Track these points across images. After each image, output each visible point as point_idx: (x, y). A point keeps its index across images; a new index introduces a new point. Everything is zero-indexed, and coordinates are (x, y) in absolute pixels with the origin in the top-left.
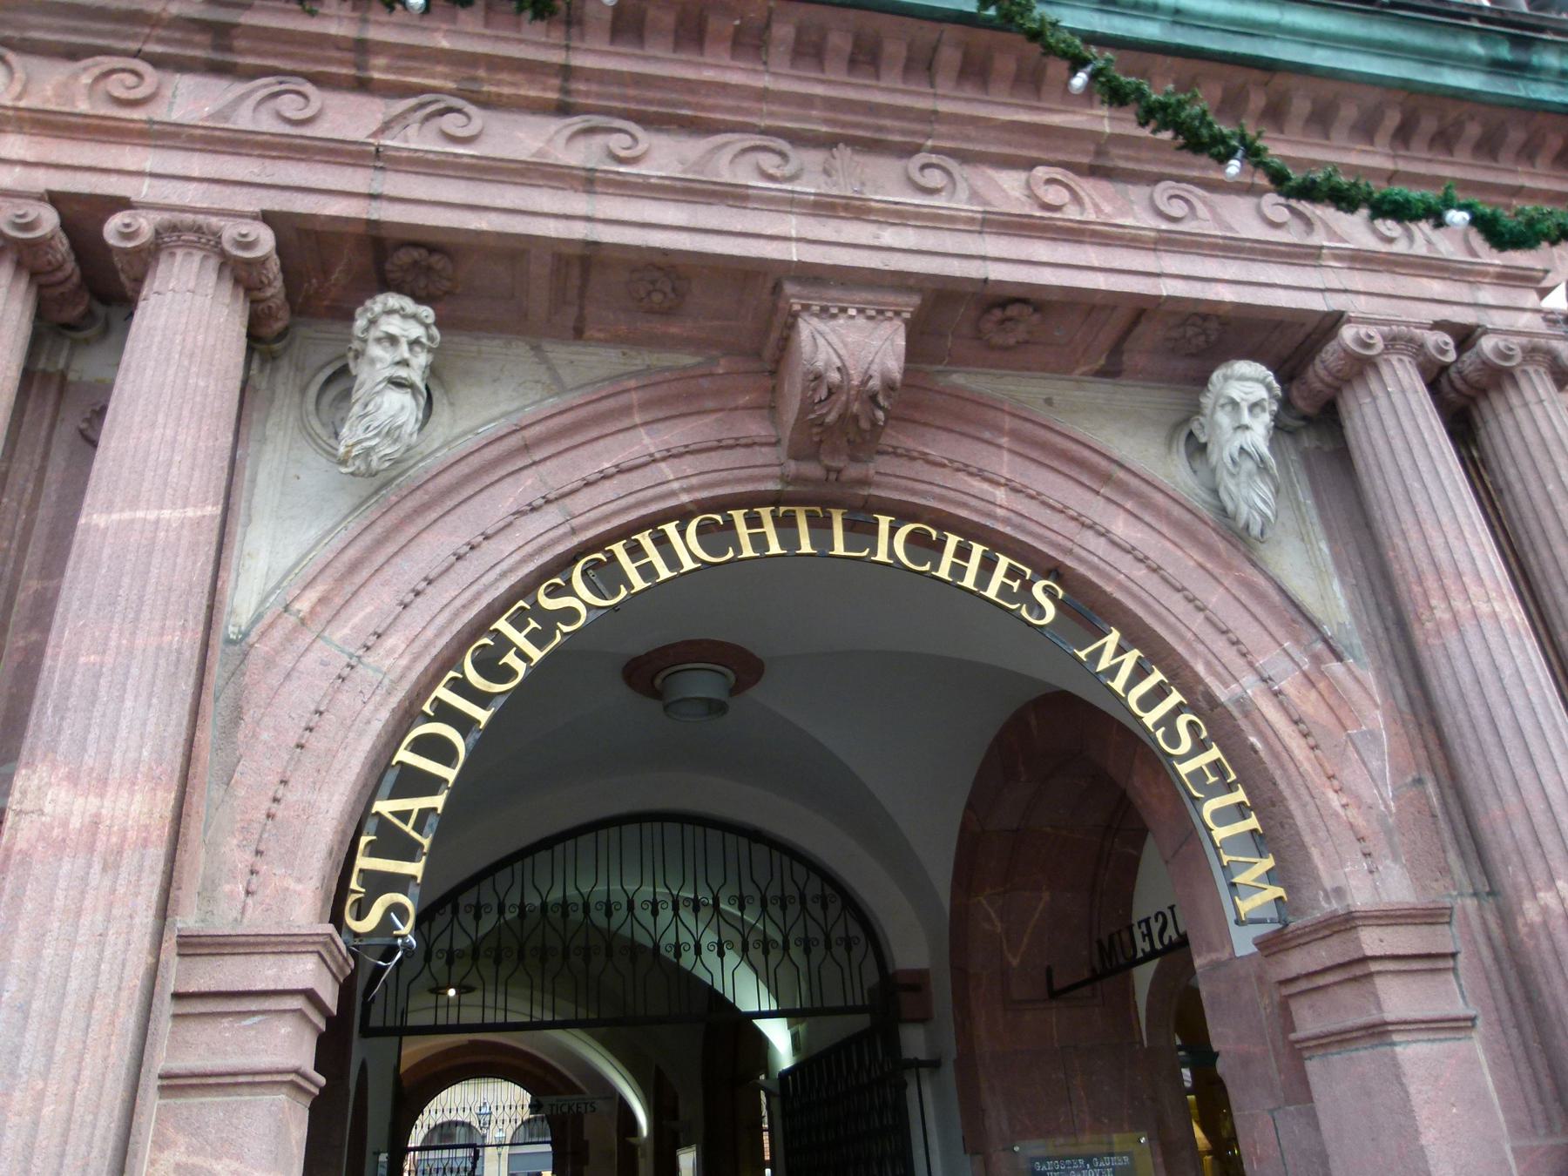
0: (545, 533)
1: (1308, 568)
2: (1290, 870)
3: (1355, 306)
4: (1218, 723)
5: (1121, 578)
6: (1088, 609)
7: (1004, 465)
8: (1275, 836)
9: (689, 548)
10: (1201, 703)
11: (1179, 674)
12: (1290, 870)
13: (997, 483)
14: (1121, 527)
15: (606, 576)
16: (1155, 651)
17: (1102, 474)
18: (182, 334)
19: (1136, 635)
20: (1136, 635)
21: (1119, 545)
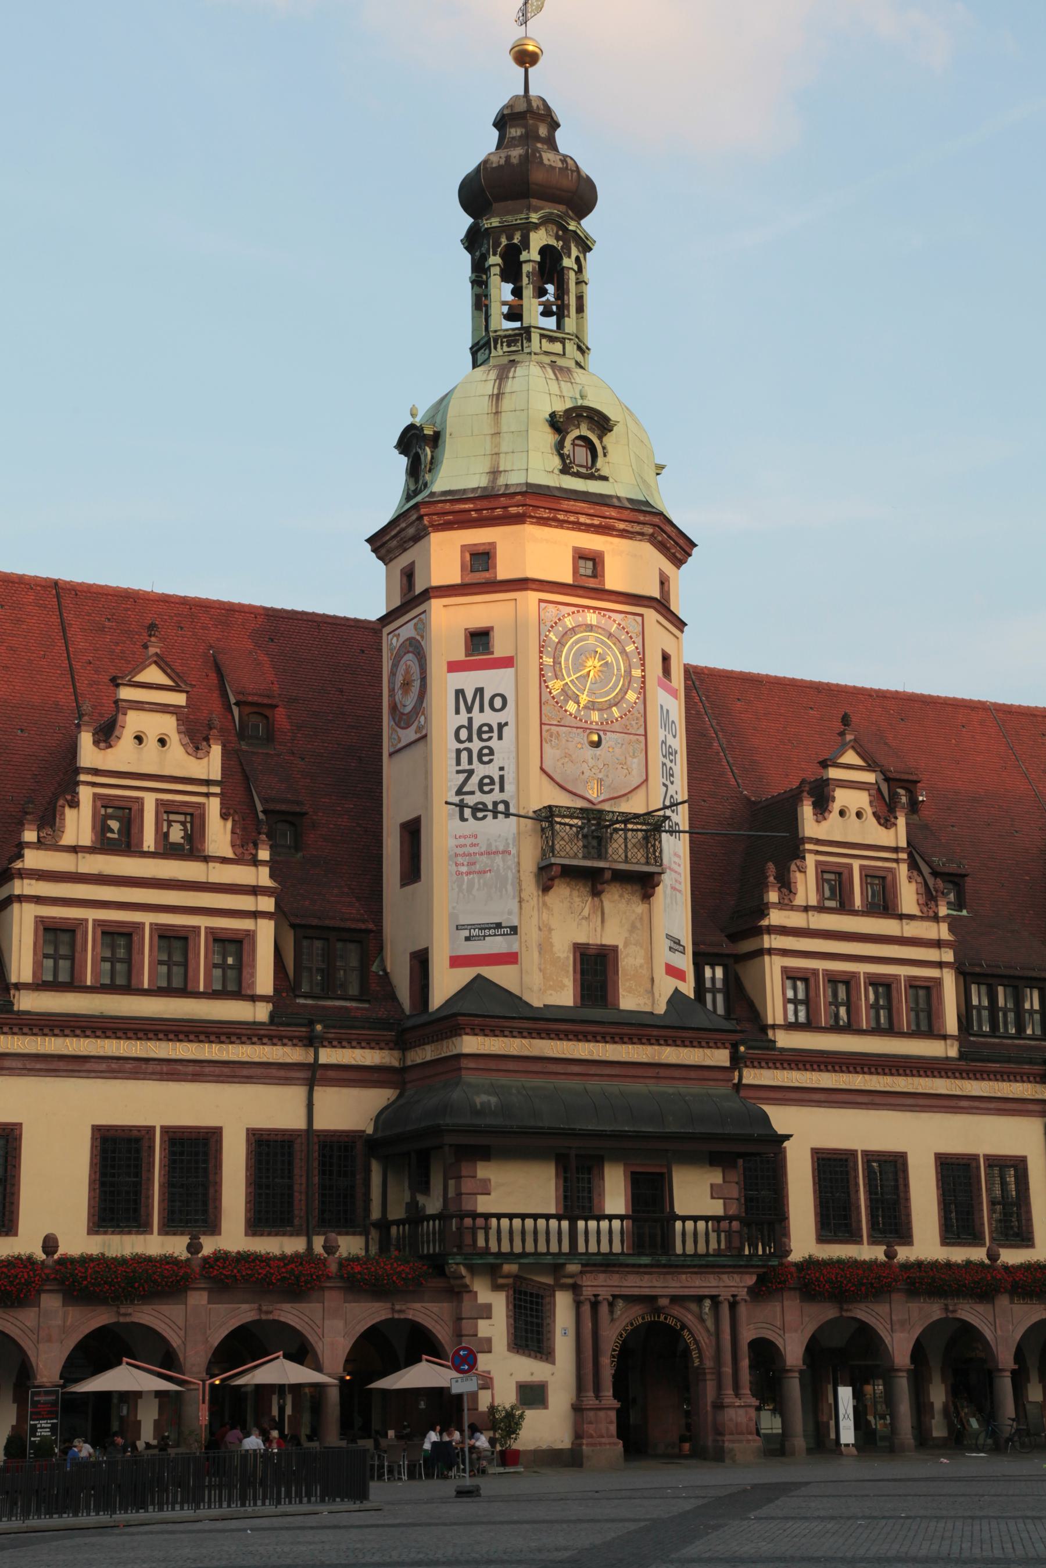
0: (627, 1320)
1: (710, 1324)
2: (701, 1361)
3: (722, 1294)
4: (696, 1342)
5: (689, 1323)
6: (684, 1326)
7: (677, 1308)
8: (700, 1357)
9: (641, 1321)
10: (695, 1339)
11: (693, 1336)
12: (701, 1361)
13: (677, 1311)
14: (690, 1317)
15: (632, 1324)
16: (690, 1333)
17: (688, 1310)
18: (604, 1309)
19: (689, 1330)
20: (689, 1330)
21: (689, 1319)
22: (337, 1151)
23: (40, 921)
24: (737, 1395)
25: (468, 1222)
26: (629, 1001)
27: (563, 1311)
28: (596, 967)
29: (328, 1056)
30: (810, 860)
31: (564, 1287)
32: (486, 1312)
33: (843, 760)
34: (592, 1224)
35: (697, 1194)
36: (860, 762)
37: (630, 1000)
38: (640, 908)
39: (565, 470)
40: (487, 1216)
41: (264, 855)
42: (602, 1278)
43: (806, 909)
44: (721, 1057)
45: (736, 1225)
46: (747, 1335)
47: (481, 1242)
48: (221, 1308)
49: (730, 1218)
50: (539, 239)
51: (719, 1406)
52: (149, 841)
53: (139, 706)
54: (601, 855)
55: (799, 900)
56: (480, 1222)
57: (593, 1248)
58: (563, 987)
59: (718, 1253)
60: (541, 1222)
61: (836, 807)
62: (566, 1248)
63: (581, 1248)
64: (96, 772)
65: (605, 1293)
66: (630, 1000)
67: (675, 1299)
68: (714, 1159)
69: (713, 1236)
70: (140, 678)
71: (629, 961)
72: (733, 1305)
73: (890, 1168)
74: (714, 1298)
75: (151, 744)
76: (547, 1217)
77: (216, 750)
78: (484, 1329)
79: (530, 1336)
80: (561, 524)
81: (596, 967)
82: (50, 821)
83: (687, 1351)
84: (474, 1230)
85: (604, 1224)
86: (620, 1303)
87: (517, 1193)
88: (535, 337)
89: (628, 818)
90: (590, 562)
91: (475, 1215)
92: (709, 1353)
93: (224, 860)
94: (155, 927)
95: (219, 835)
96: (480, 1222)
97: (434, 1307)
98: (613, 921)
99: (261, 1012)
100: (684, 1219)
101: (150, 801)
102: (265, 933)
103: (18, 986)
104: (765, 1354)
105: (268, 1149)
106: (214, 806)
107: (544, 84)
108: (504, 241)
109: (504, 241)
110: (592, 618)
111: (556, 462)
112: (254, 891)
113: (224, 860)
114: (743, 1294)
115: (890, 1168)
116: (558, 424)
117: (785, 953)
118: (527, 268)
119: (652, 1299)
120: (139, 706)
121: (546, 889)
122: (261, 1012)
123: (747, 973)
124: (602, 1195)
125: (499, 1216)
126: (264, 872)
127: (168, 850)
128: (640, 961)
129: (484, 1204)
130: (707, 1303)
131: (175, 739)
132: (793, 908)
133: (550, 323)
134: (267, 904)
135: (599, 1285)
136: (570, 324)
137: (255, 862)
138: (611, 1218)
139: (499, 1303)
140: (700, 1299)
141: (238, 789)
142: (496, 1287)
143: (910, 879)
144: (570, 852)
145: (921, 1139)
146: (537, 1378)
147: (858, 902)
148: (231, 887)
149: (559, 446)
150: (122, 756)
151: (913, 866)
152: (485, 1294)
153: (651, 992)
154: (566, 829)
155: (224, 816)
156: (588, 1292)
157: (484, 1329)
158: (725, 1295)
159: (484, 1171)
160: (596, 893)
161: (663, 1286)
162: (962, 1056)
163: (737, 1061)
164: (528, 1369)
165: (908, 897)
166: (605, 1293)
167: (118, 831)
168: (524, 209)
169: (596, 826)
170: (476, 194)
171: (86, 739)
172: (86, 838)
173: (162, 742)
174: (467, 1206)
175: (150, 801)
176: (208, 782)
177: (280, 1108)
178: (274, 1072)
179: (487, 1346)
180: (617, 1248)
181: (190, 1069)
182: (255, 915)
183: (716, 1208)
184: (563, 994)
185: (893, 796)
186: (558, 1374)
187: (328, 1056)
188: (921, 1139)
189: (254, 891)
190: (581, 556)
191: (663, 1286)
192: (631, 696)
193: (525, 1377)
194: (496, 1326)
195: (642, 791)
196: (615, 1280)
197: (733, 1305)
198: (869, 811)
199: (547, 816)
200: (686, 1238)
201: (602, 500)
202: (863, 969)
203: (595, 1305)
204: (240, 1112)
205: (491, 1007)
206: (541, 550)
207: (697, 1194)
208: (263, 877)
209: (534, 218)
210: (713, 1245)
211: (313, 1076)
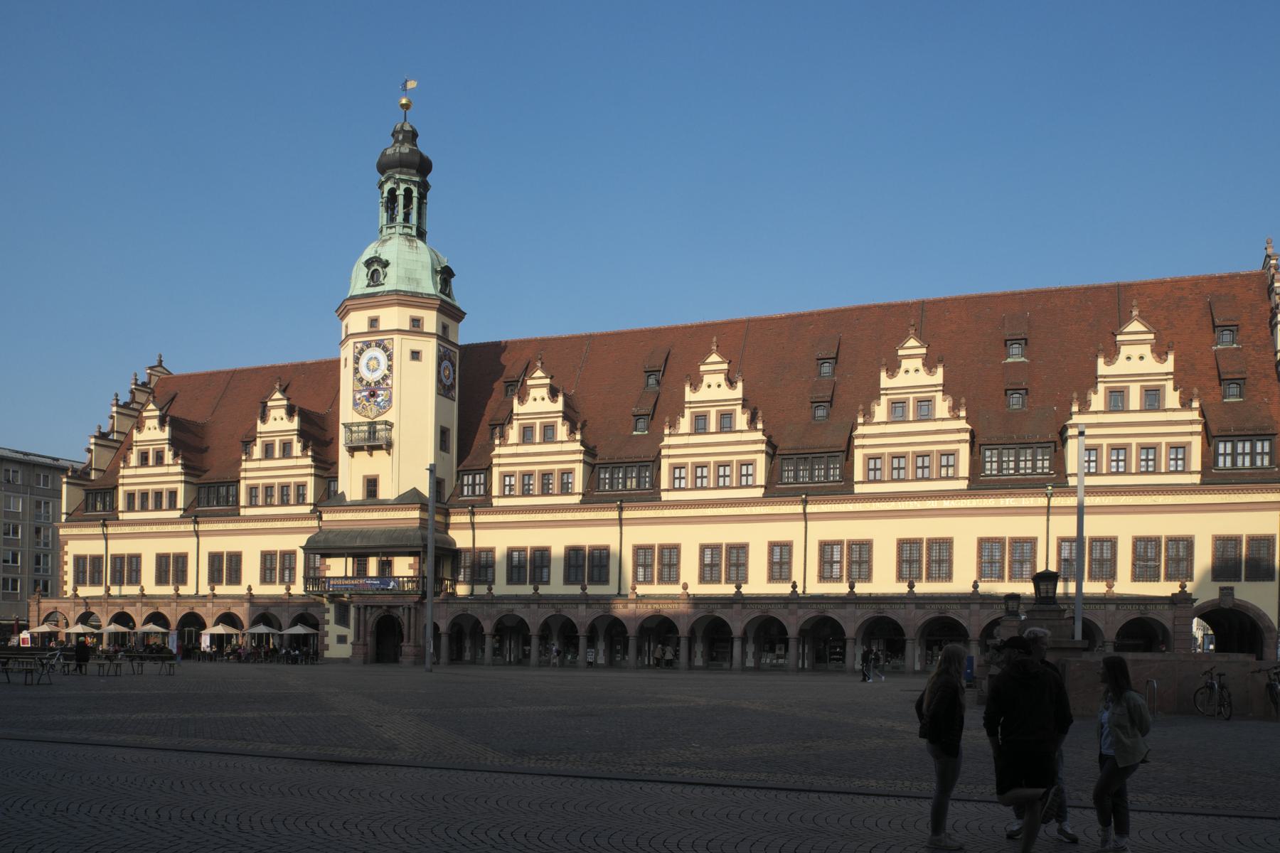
13: (394, 611)
28: (372, 485)
32: (328, 610)
39: (368, 286)
78: (327, 616)
79: (342, 620)
81: (372, 485)
82: (249, 454)
102: (310, 482)
121: (352, 456)
129: (328, 574)
139: (332, 607)
148: (300, 468)
157: (327, 616)
164: (342, 630)
179: (328, 622)
186: (350, 633)
190: (374, 322)
194: (331, 616)
202: (536, 468)
203: (358, 609)
207: (403, 567)
208: (309, 461)
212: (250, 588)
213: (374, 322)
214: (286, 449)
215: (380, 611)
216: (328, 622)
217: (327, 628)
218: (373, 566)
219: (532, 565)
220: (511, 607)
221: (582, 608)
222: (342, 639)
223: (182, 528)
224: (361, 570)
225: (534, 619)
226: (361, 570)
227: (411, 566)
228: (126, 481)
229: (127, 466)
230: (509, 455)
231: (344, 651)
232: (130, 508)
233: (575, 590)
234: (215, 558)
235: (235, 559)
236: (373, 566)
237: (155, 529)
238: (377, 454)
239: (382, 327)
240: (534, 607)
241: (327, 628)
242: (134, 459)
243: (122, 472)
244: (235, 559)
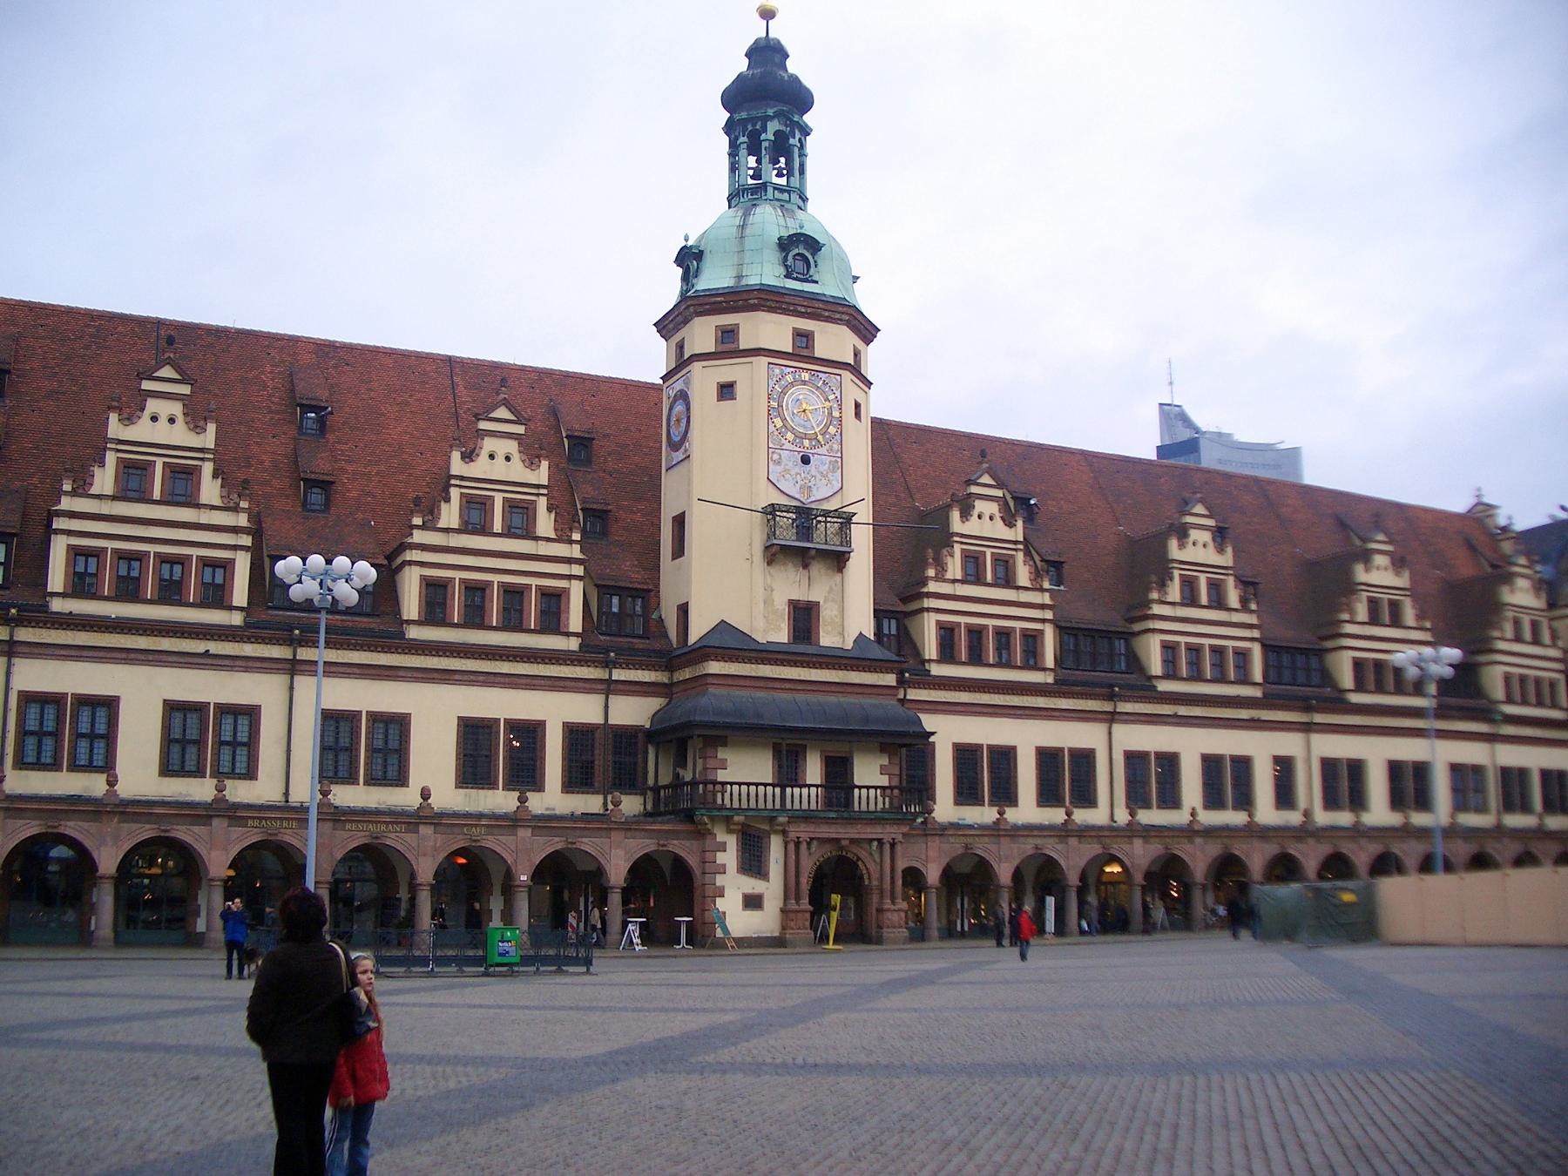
1: (877, 857)
13: (854, 849)
18: (804, 846)
21: (863, 854)
22: (625, 738)
23: (423, 578)
24: (893, 903)
25: (710, 787)
26: (827, 639)
27: (776, 850)
28: (804, 616)
29: (618, 674)
30: (957, 548)
31: (776, 832)
33: (981, 481)
34: (797, 790)
35: (869, 772)
36: (992, 482)
37: (827, 639)
38: (838, 577)
40: (724, 784)
41: (576, 536)
42: (803, 827)
43: (954, 581)
44: (890, 679)
45: (896, 792)
46: (901, 864)
47: (719, 801)
48: (542, 840)
49: (891, 788)
50: (773, 126)
51: (880, 911)
52: (498, 526)
53: (493, 434)
54: (809, 539)
55: (949, 576)
56: (719, 787)
57: (797, 806)
58: (780, 629)
59: (883, 810)
60: (761, 788)
61: (976, 513)
62: (778, 806)
63: (789, 806)
64: (462, 478)
65: (804, 836)
66: (827, 639)
67: (852, 841)
68: (884, 749)
69: (880, 799)
70: (497, 414)
71: (827, 613)
72: (893, 845)
73: (1004, 757)
74: (879, 840)
75: (500, 462)
76: (765, 785)
77: (545, 464)
78: (721, 858)
79: (753, 864)
80: (785, 312)
81: (804, 616)
83: (861, 877)
84: (714, 794)
85: (805, 791)
86: (815, 843)
87: (745, 770)
88: (770, 190)
89: (826, 513)
90: (804, 339)
91: (715, 783)
92: (875, 876)
93: (548, 540)
94: (502, 585)
95: (545, 523)
96: (719, 787)
97: (688, 843)
98: (816, 587)
99: (573, 644)
100: (860, 787)
101: (499, 500)
102: (576, 591)
103: (409, 622)
104: (914, 878)
105: (577, 736)
106: (542, 503)
107: (778, 31)
108: (750, 128)
109: (750, 128)
110: (806, 376)
111: (782, 271)
112: (569, 561)
113: (548, 540)
114: (900, 838)
115: (1004, 757)
116: (785, 244)
117: (938, 611)
118: (765, 144)
119: (838, 840)
120: (493, 434)
122: (573, 644)
123: (912, 624)
124: (804, 772)
125: (732, 784)
126: (577, 548)
127: (508, 533)
128: (836, 612)
129: (722, 776)
130: (875, 843)
131: (516, 457)
132: (945, 581)
133: (783, 181)
134: (578, 570)
135: (801, 831)
136: (795, 181)
137: (571, 542)
138: (809, 786)
139: (732, 842)
140: (872, 840)
141: (561, 497)
142: (730, 831)
143: (1025, 562)
144: (788, 537)
145: (1026, 738)
146: (757, 891)
147: (989, 578)
148: (551, 557)
149: (785, 259)
150: (480, 468)
151: (1027, 553)
152: (721, 836)
153: (842, 634)
154: (785, 520)
155: (549, 509)
156: (792, 836)
157: (721, 858)
158: (887, 838)
159: (722, 753)
160: (806, 566)
161: (845, 832)
162: (1056, 682)
163: (901, 682)
164: (752, 885)
165: (1023, 575)
166: (804, 836)
167: (476, 518)
168: (766, 109)
169: (805, 517)
170: (734, 98)
171: (456, 456)
172: (455, 524)
173: (508, 459)
174: (710, 777)
175: (499, 500)
176: (538, 486)
177: (585, 709)
178: (580, 684)
179: (722, 870)
180: (813, 806)
181: (524, 681)
182: (570, 577)
183: (884, 781)
184: (780, 634)
185: (1018, 507)
186: (772, 889)
187: (618, 674)
188: (1026, 738)
189: (569, 561)
191: (845, 832)
192: (832, 430)
193: (749, 891)
194: (729, 857)
195: (838, 496)
196: (811, 828)
197: (893, 845)
198: (998, 515)
199: (771, 511)
200: (862, 800)
201: (813, 297)
203: (798, 844)
204: (558, 711)
205: (730, 643)
206: (772, 330)
208: (575, 551)
209: (770, 112)
210: (880, 806)
211: (609, 688)
212: (425, 794)
213: (804, 338)
214: (520, 521)
215: (828, 847)
216: (722, 870)
217: (720, 880)
218: (814, 770)
219: (986, 773)
220: (1039, 841)
221: (1138, 843)
222: (753, 902)
223: (249, 650)
224: (789, 775)
225: (1072, 860)
226: (789, 775)
227: (883, 770)
228: (76, 525)
229: (81, 490)
230: (950, 596)
231: (765, 922)
232: (81, 585)
233: (1056, 816)
234: (336, 723)
235: (394, 727)
236: (814, 770)
237: (166, 644)
238: (817, 569)
239: (819, 352)
240: (1073, 841)
241: (720, 880)
242: (104, 479)
243: (66, 503)
244: (394, 727)
